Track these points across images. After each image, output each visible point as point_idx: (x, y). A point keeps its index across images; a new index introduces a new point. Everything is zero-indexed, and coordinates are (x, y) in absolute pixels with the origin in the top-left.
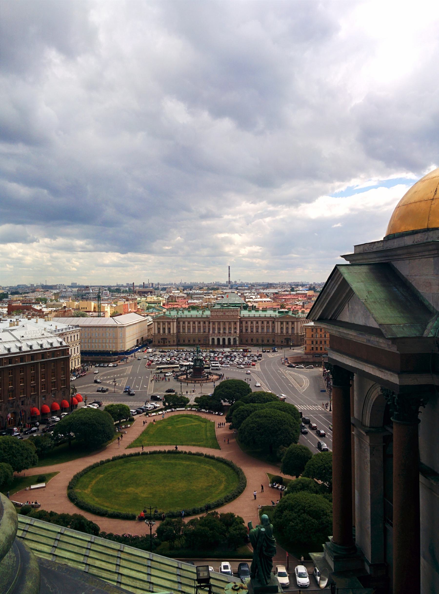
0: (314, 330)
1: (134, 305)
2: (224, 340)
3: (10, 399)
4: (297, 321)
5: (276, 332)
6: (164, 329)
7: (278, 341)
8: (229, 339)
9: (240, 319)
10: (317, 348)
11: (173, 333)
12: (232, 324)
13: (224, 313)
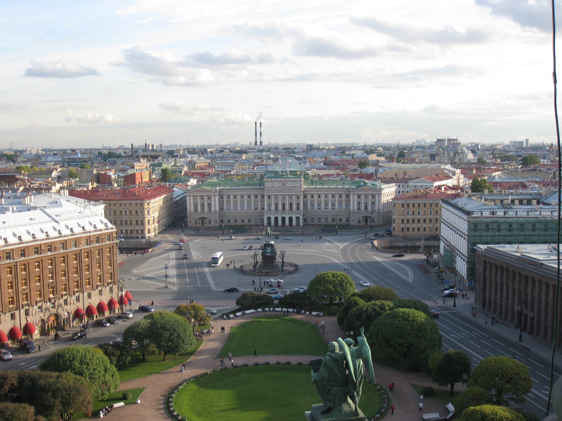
1: (148, 173)
2: (283, 219)
3: (51, 296)
5: (352, 208)
6: (203, 205)
8: (291, 219)
10: (408, 228)
11: (215, 211)
12: (294, 198)
13: (283, 184)
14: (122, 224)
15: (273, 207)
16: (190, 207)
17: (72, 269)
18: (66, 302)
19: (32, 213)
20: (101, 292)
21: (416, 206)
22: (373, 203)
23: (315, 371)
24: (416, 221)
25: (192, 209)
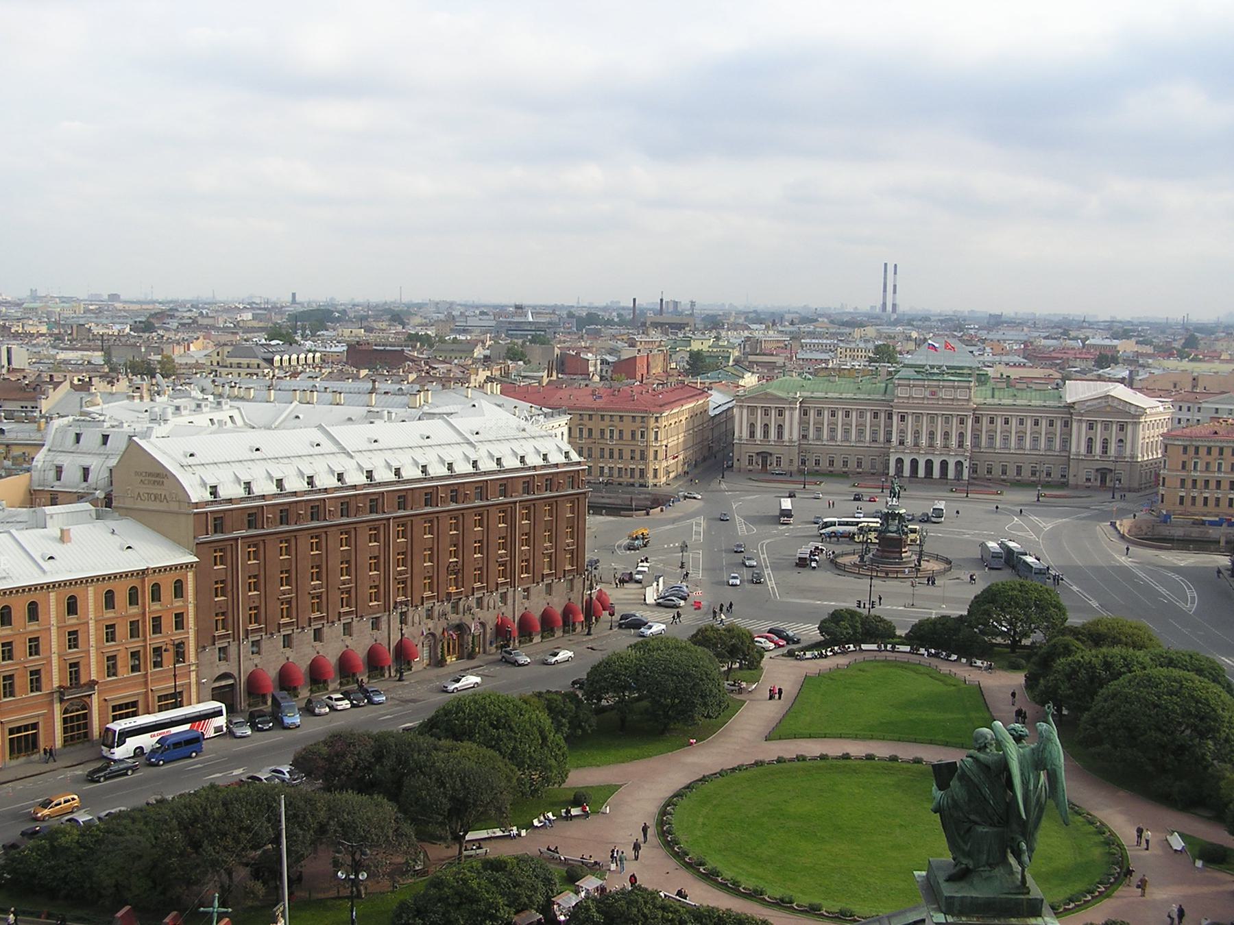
0: (1191, 451)
3: (453, 589)
4: (1137, 424)
5: (1073, 450)
7: (1078, 474)
8: (944, 464)
9: (975, 410)
10: (1194, 498)
11: (791, 441)
13: (933, 393)
14: (602, 457)
15: (909, 440)
16: (741, 431)
17: (495, 540)
18: (479, 602)
19: (426, 426)
20: (549, 586)
21: (1215, 452)
22: (1121, 441)
23: (940, 788)
24: (1213, 484)
25: (745, 434)
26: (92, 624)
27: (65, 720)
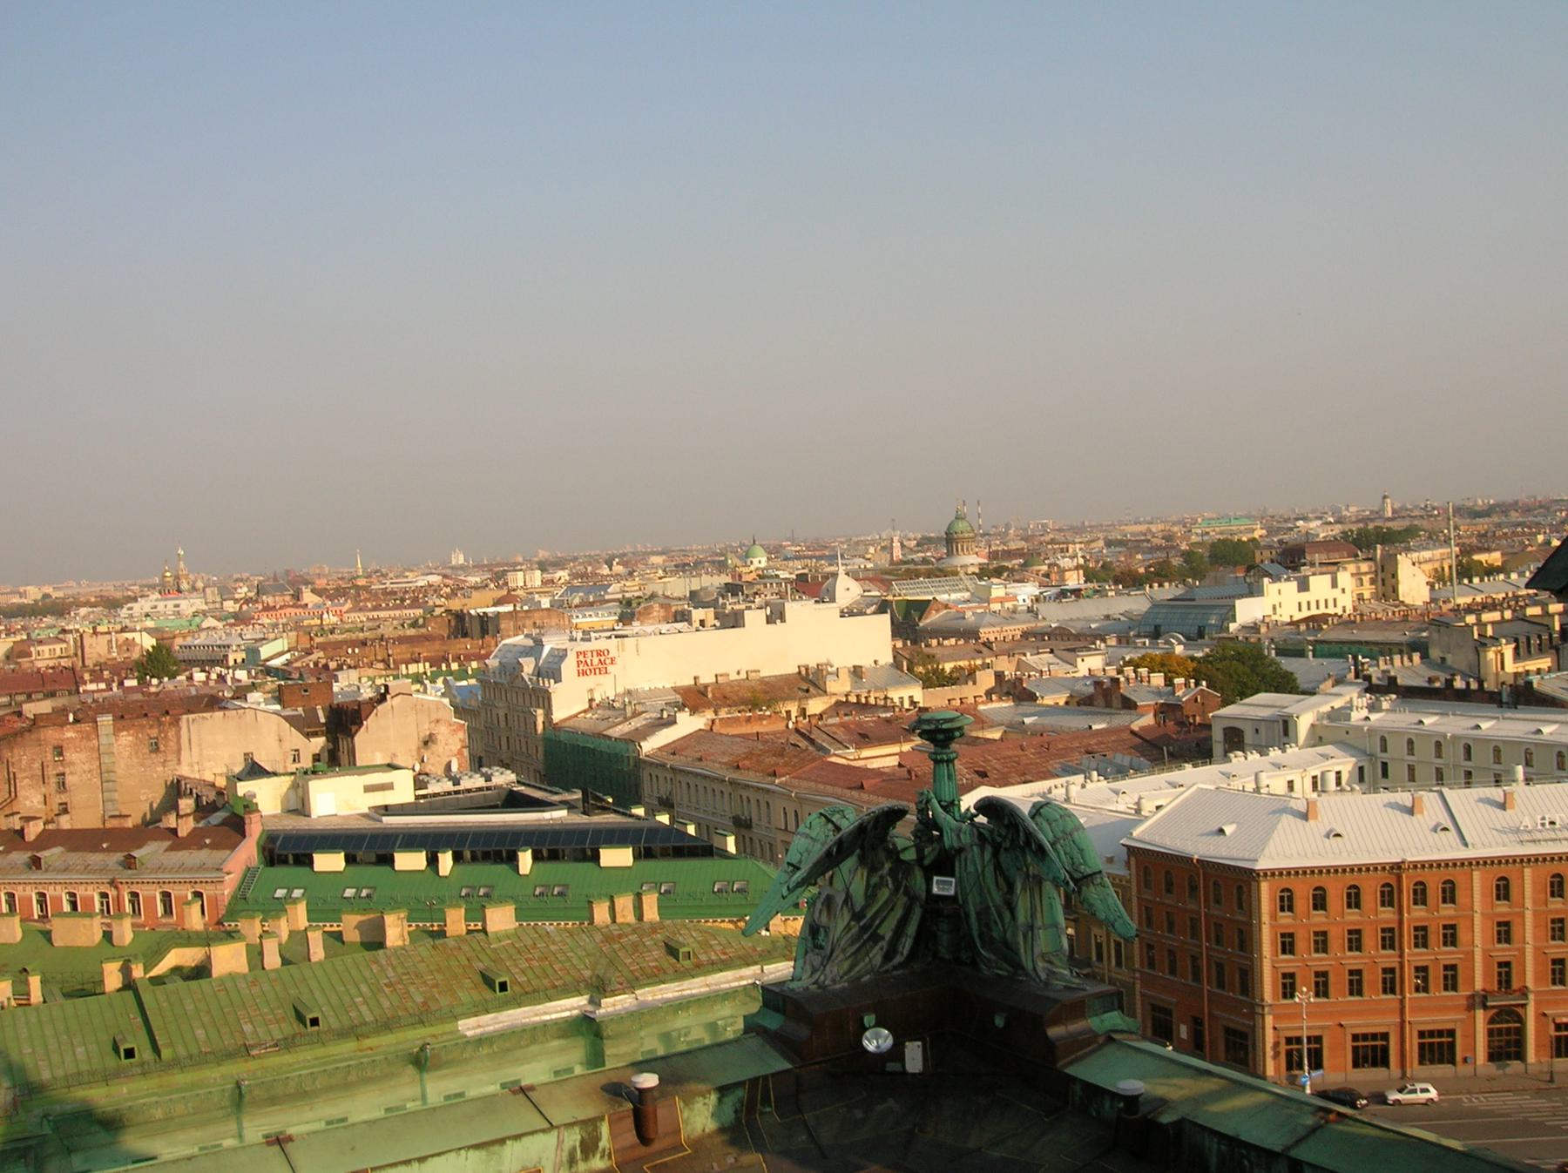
26: (1529, 915)
27: (1490, 1033)
